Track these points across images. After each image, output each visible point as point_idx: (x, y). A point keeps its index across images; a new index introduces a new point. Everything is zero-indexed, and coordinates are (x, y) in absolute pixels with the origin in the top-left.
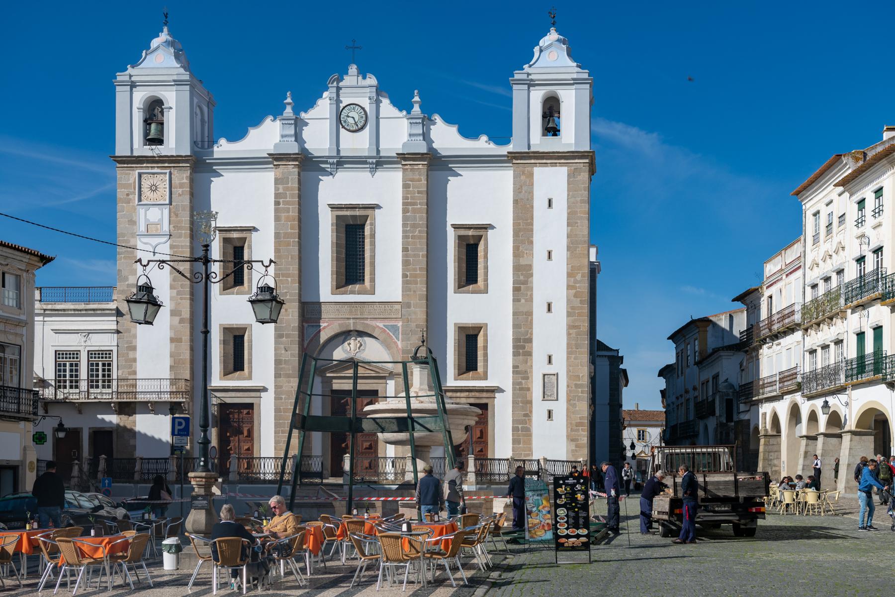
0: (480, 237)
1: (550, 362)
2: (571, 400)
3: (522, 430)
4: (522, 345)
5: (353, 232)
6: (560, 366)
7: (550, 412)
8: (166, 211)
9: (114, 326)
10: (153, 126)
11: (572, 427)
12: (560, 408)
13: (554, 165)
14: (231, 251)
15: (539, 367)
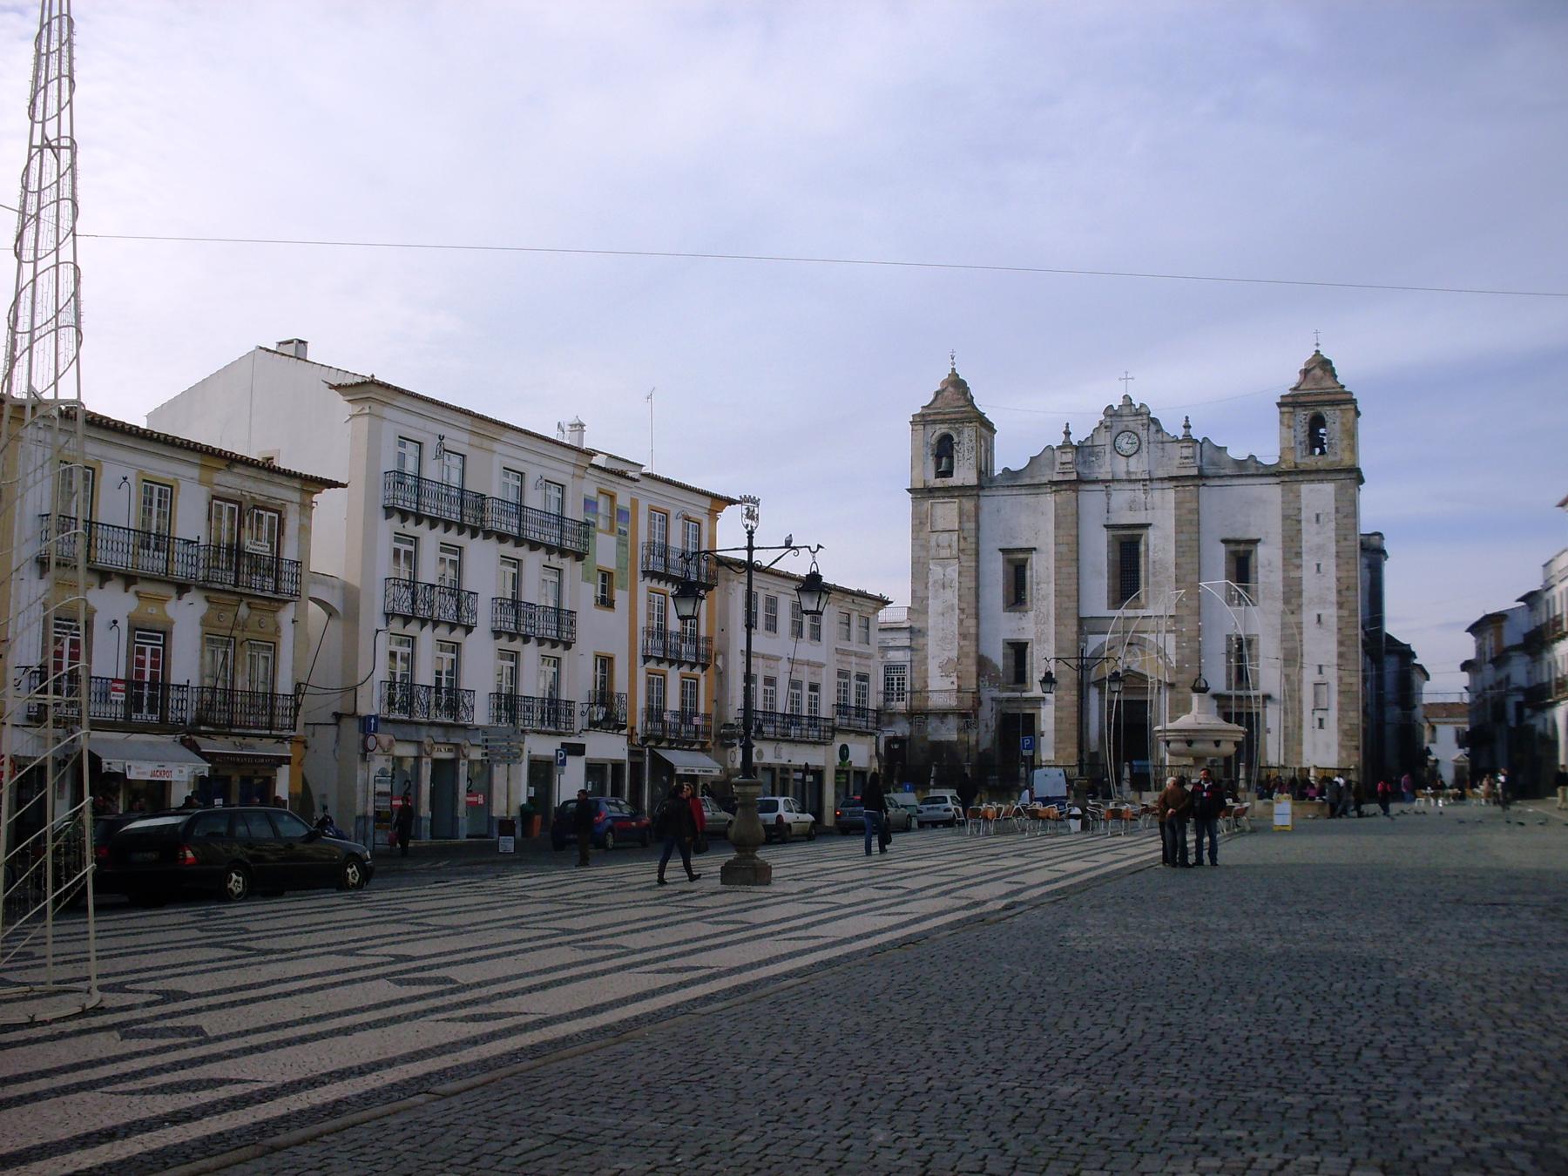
0: (1249, 553)
1: (1320, 672)
2: (1342, 708)
3: (1292, 738)
4: (1292, 658)
5: (1127, 553)
6: (1331, 675)
7: (1321, 720)
8: (955, 537)
9: (907, 643)
10: (944, 460)
11: (1345, 734)
12: (1332, 717)
13: (1321, 481)
14: (1012, 569)
15: (1310, 676)
